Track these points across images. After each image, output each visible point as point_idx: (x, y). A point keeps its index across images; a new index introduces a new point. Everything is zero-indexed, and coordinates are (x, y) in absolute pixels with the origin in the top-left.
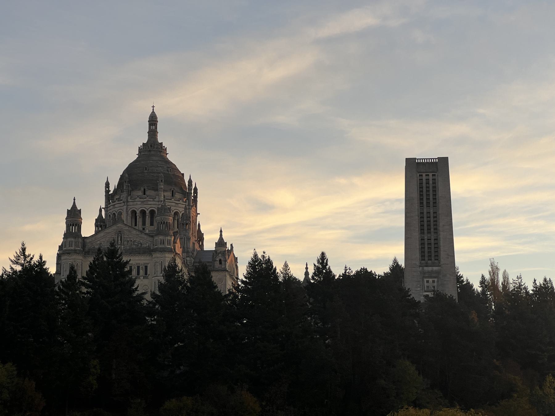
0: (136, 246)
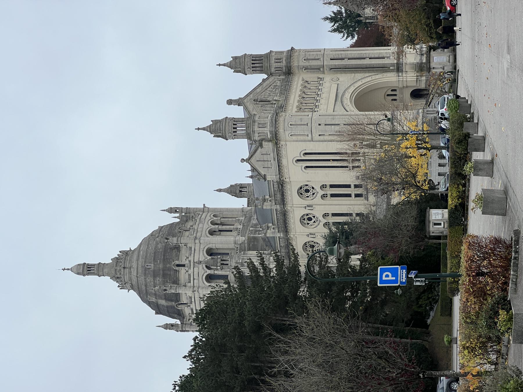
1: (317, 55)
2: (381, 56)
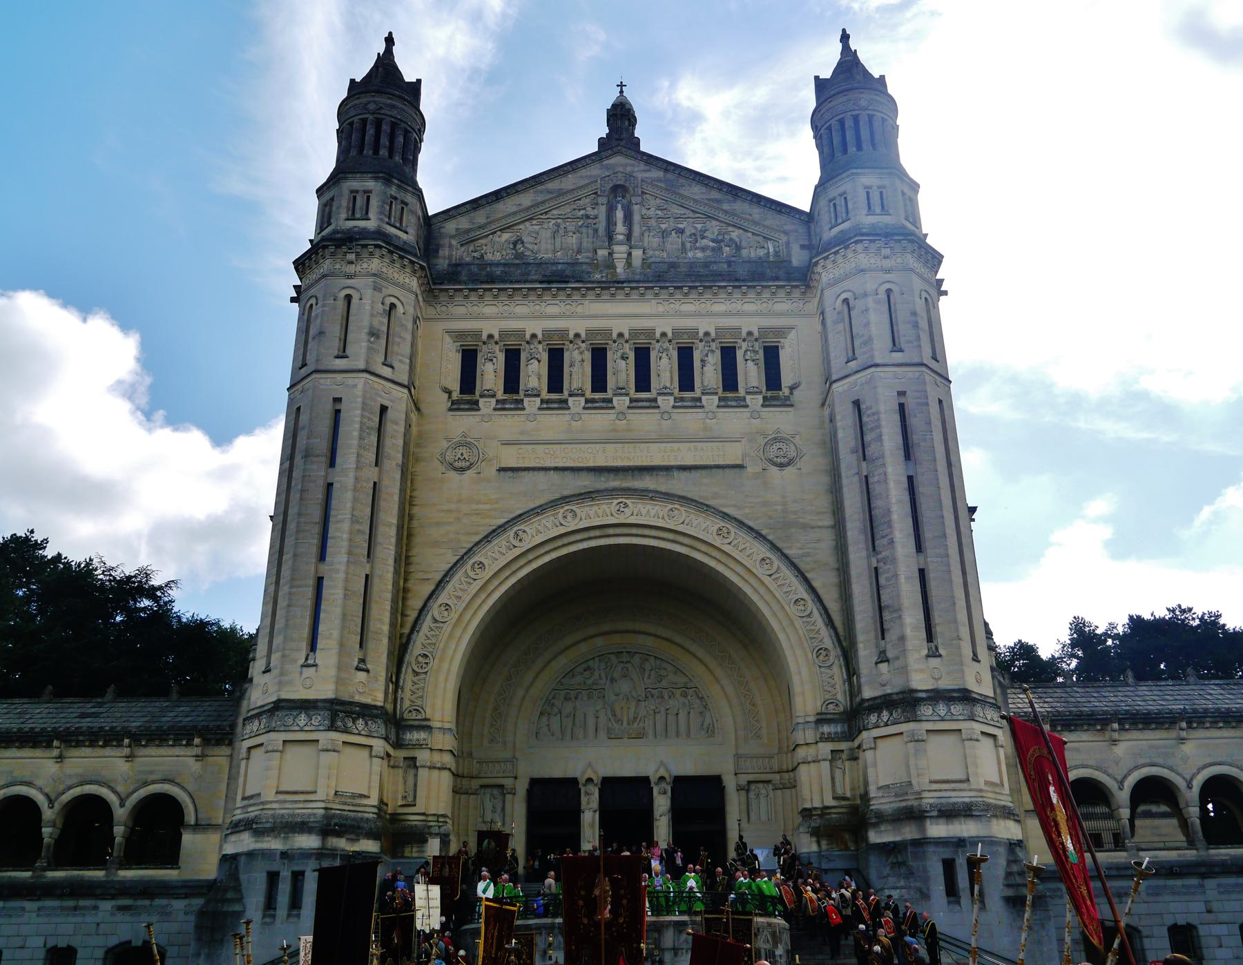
0: (708, 253)
2: (887, 616)
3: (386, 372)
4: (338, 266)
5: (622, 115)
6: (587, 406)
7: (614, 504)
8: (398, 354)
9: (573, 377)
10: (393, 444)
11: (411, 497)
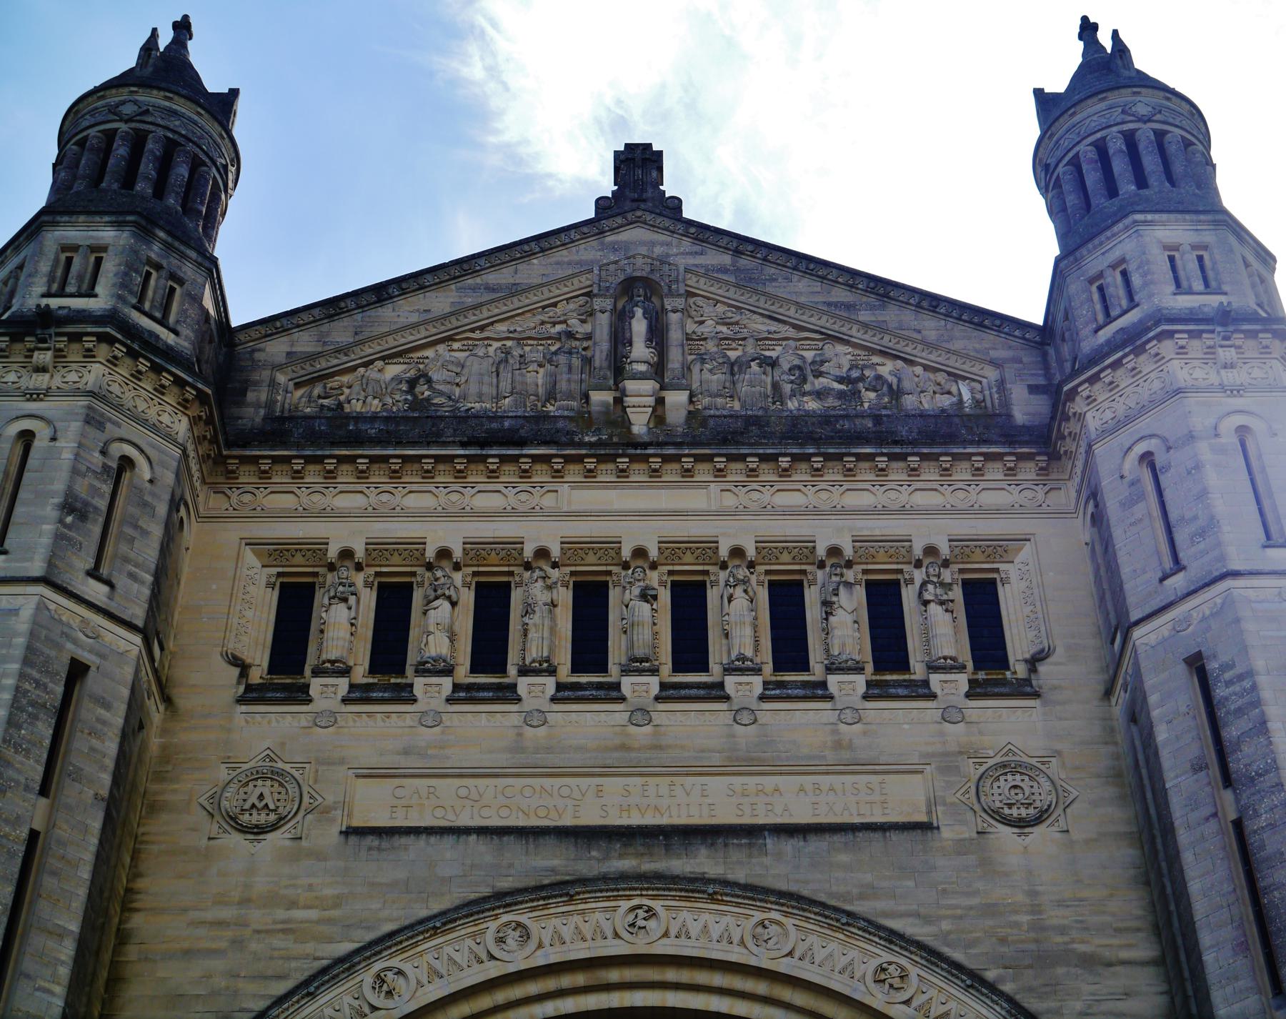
1: (1209, 528)
3: (96, 591)
4: (12, 377)
5: (644, 160)
6: (560, 695)
7: (621, 911)
8: (126, 560)
9: (530, 636)
10: (92, 749)
11: (129, 891)
